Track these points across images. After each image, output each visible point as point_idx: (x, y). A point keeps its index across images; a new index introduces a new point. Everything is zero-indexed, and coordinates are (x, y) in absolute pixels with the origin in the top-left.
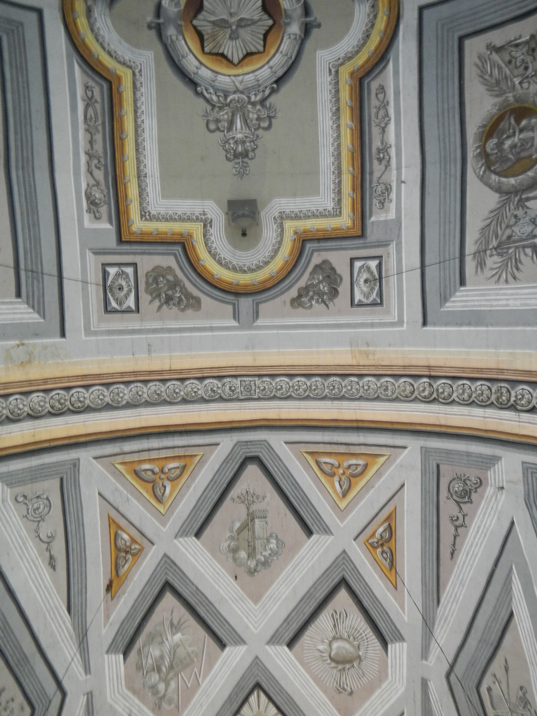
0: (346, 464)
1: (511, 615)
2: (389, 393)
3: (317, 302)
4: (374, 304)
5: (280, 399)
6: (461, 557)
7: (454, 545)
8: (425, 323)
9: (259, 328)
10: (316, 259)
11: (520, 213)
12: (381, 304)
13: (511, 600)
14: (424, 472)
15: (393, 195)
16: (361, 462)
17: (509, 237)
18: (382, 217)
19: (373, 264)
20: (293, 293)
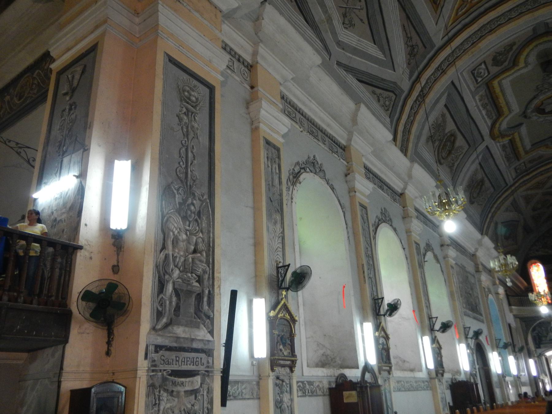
0: (468, 5)
1: (375, 44)
2: (457, 50)
3: (502, 51)
4: (474, 70)
5: (514, 8)
6: (401, 29)
7: (405, 32)
8: (452, 83)
9: (532, 26)
10: (506, 63)
11: (439, 138)
12: (472, 72)
13: (378, 48)
14: (430, 39)
15: (478, 101)
16: (460, 13)
17: (439, 130)
18: (480, 94)
19: (479, 79)
20: (515, 48)
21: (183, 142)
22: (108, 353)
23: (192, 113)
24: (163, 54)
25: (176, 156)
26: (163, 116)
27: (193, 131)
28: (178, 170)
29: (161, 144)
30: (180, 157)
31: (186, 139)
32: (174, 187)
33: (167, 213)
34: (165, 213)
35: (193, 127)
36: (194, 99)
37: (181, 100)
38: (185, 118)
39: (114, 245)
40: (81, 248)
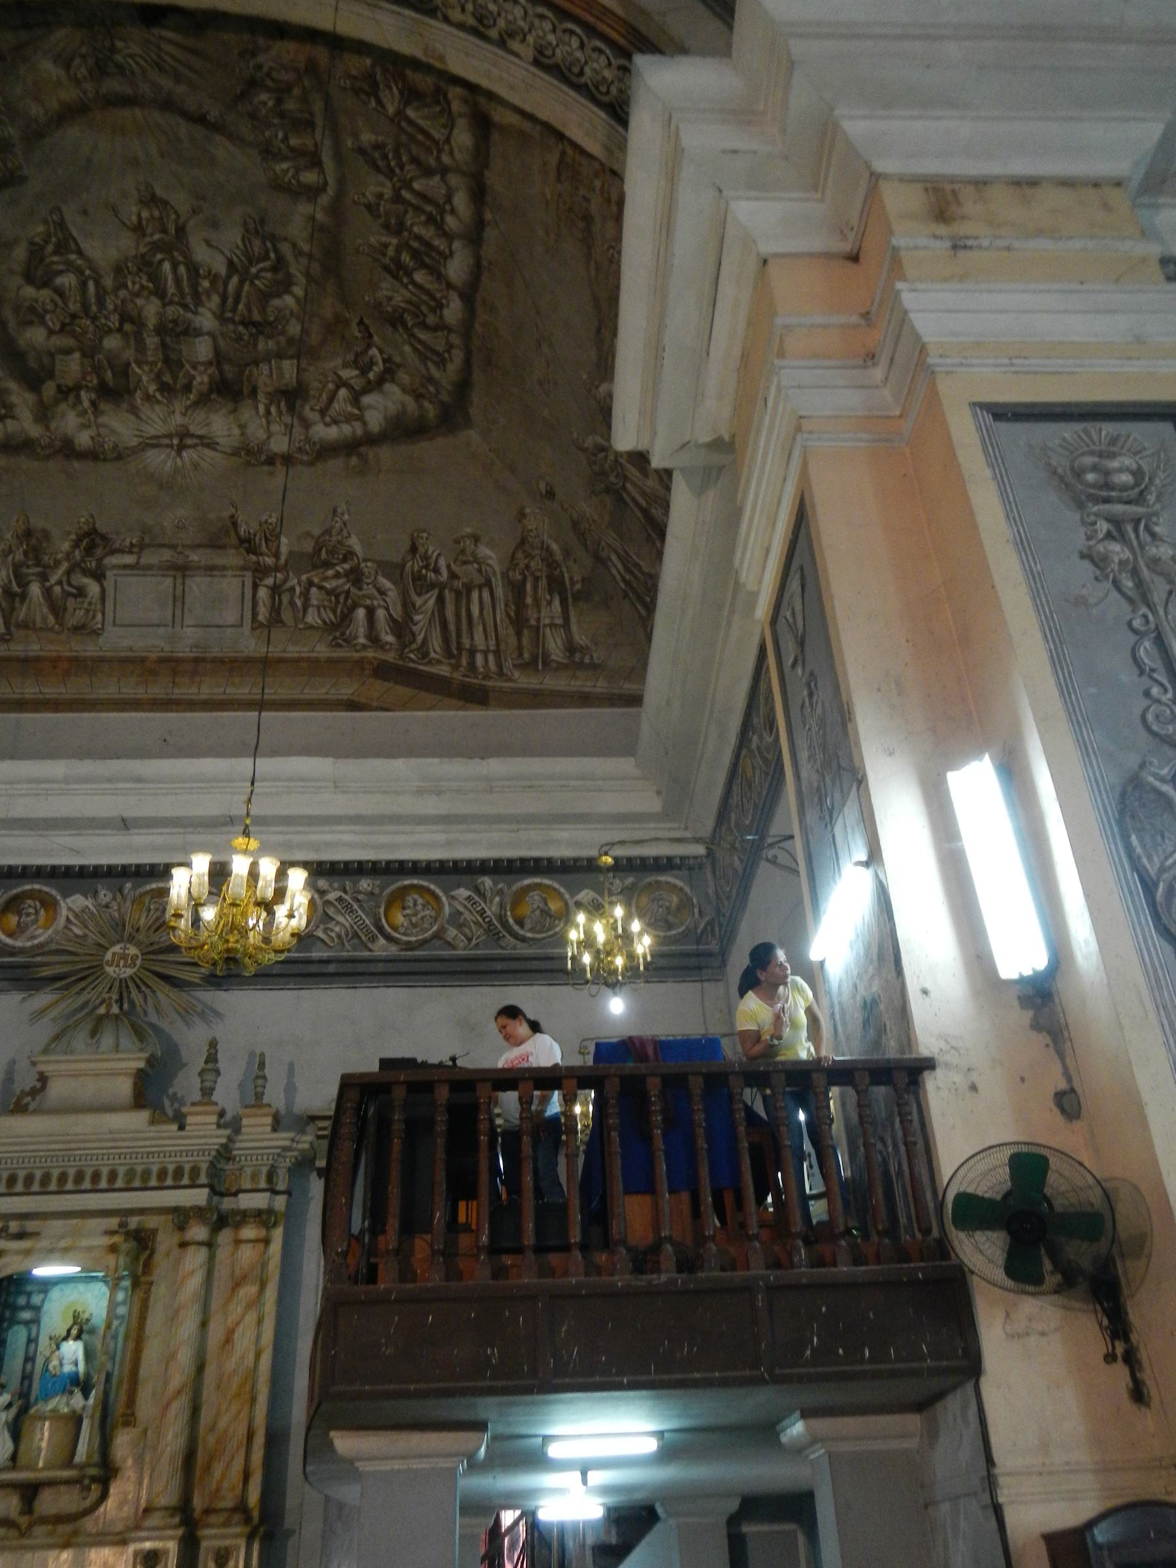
21: (1137, 623)
22: (1138, 1394)
23: (1136, 522)
24: (967, 412)
25: (1127, 676)
26: (1036, 581)
27: (1161, 574)
28: (1150, 717)
29: (1057, 661)
30: (1142, 673)
31: (1144, 610)
32: (1155, 775)
33: (1162, 870)
34: (1153, 872)
35: (1154, 563)
36: (1125, 478)
37: (1080, 506)
38: (1116, 547)
39: (1036, 1026)
40: (928, 1064)
